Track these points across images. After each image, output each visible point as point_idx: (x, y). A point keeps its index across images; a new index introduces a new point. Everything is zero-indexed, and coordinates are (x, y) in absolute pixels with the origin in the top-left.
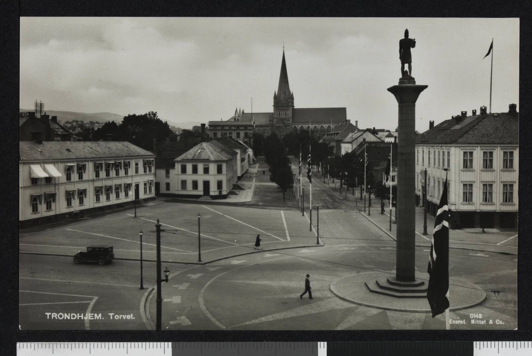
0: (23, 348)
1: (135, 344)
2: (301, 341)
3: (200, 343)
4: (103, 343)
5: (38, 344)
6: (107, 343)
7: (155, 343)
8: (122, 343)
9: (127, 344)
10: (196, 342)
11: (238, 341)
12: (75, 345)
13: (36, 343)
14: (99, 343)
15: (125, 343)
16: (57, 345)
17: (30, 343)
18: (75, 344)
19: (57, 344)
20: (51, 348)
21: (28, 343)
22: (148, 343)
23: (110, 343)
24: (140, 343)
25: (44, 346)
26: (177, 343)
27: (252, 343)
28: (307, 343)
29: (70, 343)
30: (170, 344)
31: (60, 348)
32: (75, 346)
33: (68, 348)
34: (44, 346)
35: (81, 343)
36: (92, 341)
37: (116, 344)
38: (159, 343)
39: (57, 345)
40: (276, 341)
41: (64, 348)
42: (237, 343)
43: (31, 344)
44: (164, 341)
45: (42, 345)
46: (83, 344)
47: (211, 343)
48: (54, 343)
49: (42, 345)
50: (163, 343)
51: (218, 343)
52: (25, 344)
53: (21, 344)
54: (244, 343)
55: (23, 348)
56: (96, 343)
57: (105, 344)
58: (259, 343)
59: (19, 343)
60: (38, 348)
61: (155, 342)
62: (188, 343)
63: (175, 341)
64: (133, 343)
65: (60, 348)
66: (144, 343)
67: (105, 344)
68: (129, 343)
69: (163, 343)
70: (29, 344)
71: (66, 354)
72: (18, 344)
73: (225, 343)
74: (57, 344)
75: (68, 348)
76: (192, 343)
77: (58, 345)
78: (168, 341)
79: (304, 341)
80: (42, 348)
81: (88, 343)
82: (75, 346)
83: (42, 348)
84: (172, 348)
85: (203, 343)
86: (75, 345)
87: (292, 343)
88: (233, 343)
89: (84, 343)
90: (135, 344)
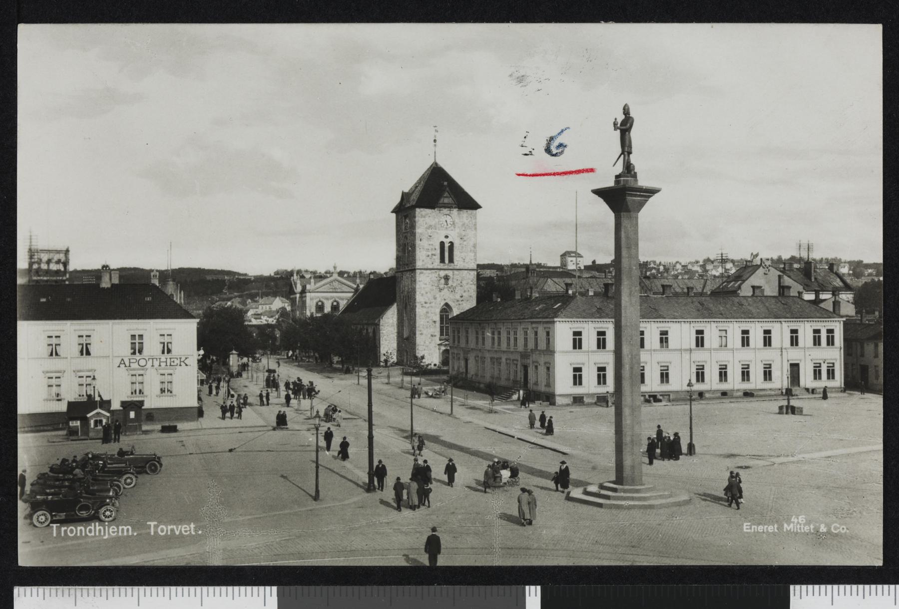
0: (25, 596)
1: (214, 590)
2: (497, 584)
3: (325, 588)
4: (161, 588)
5: (50, 589)
6: (167, 588)
7: (249, 588)
8: (192, 588)
9: (202, 589)
10: (318, 585)
11: (390, 584)
12: (113, 590)
13: (47, 588)
14: (154, 588)
15: (198, 588)
16: (82, 592)
17: (36, 587)
18: (113, 589)
19: (82, 589)
20: (73, 597)
21: (33, 587)
22: (236, 588)
23: (173, 588)
24: (224, 588)
25: (60, 592)
26: (287, 588)
27: (413, 588)
28: (507, 587)
29: (104, 588)
30: (275, 588)
31: (88, 596)
32: (113, 593)
33: (101, 596)
34: (60, 592)
35: (123, 588)
36: (141, 585)
37: (183, 590)
38: (255, 588)
39: (82, 592)
40: (453, 585)
41: (95, 596)
42: (388, 588)
43: (38, 589)
44: (264, 585)
45: (57, 592)
46: (126, 589)
47: (344, 588)
48: (77, 587)
49: (57, 592)
50: (262, 588)
51: (356, 588)
52: (28, 589)
53: (22, 589)
54: (400, 588)
55: (25, 596)
56: (148, 588)
57: (164, 590)
58: (425, 588)
59: (17, 587)
60: (50, 596)
61: (249, 585)
62: (306, 588)
63: (282, 585)
64: (211, 588)
65: (88, 596)
66: (230, 588)
67: (164, 590)
68: (205, 588)
69: (263, 587)
70: (35, 589)
71: (97, 607)
72: (17, 590)
73: (369, 588)
74: (82, 589)
75: (101, 596)
76: (312, 588)
77: (84, 591)
78: (271, 584)
79: (502, 584)
80: (57, 596)
81: (136, 588)
82: (113, 593)
83: (57, 596)
84: (278, 596)
85: (331, 588)
86: (113, 590)
87: (482, 588)
88: (381, 588)
89: (129, 588)
90: (214, 590)
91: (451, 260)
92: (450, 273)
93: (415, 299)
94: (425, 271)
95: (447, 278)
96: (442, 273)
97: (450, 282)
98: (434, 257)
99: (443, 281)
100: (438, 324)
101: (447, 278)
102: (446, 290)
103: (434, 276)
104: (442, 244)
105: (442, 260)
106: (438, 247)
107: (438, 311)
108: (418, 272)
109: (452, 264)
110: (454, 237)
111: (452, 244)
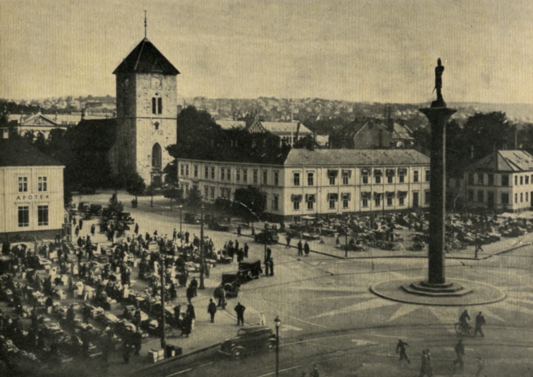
91: (160, 112)
92: (159, 121)
93: (136, 139)
94: (142, 119)
95: (157, 125)
96: (154, 121)
97: (160, 127)
98: (149, 109)
99: (154, 127)
100: (151, 158)
101: (157, 125)
102: (156, 133)
103: (148, 122)
104: (154, 99)
105: (154, 112)
106: (150, 100)
107: (151, 147)
108: (138, 119)
109: (160, 114)
110: (162, 94)
111: (160, 100)
